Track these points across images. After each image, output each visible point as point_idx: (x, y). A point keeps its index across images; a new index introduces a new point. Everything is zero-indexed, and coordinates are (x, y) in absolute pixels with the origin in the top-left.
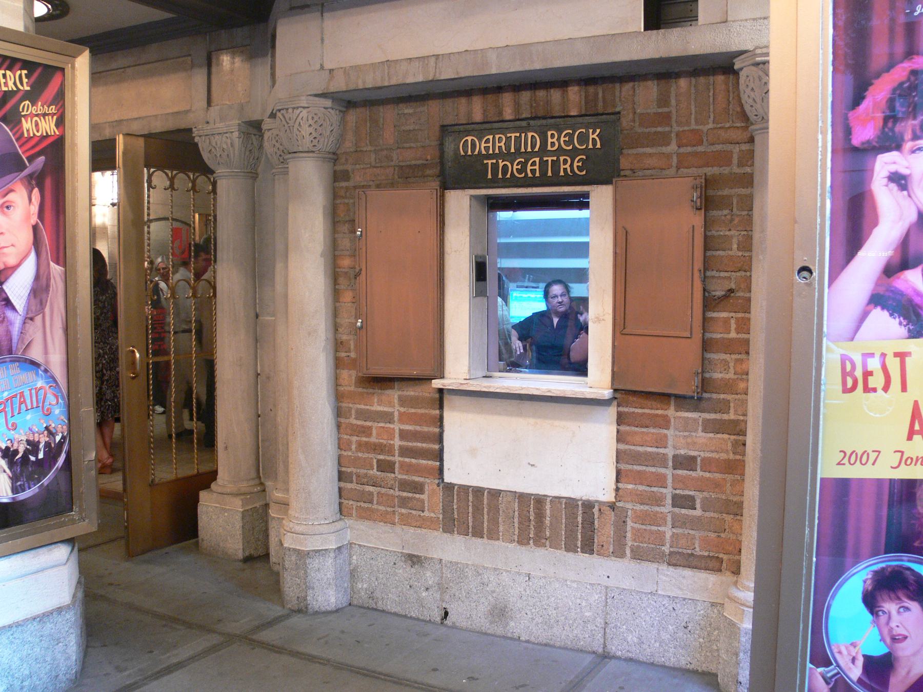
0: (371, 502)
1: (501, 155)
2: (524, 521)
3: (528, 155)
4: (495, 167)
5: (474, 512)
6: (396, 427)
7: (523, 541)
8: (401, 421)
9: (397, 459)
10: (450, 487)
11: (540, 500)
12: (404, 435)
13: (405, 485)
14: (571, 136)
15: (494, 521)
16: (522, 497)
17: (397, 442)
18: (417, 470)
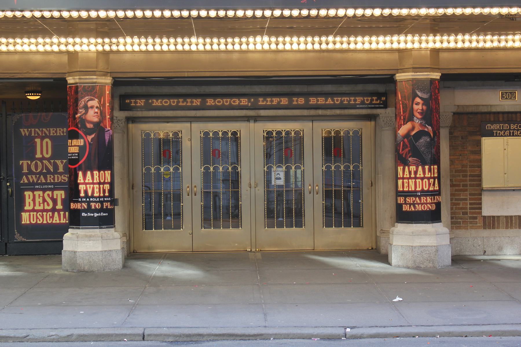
0: (463, 222)
1: (498, 130)
2: (507, 222)
3: (506, 130)
4: (496, 133)
5: (492, 223)
6: (468, 202)
7: (507, 228)
8: (470, 200)
9: (469, 211)
10: (485, 217)
11: (511, 217)
12: (471, 204)
13: (471, 218)
14: (517, 126)
15: (499, 224)
16: (506, 217)
17: (469, 206)
18: (475, 213)
